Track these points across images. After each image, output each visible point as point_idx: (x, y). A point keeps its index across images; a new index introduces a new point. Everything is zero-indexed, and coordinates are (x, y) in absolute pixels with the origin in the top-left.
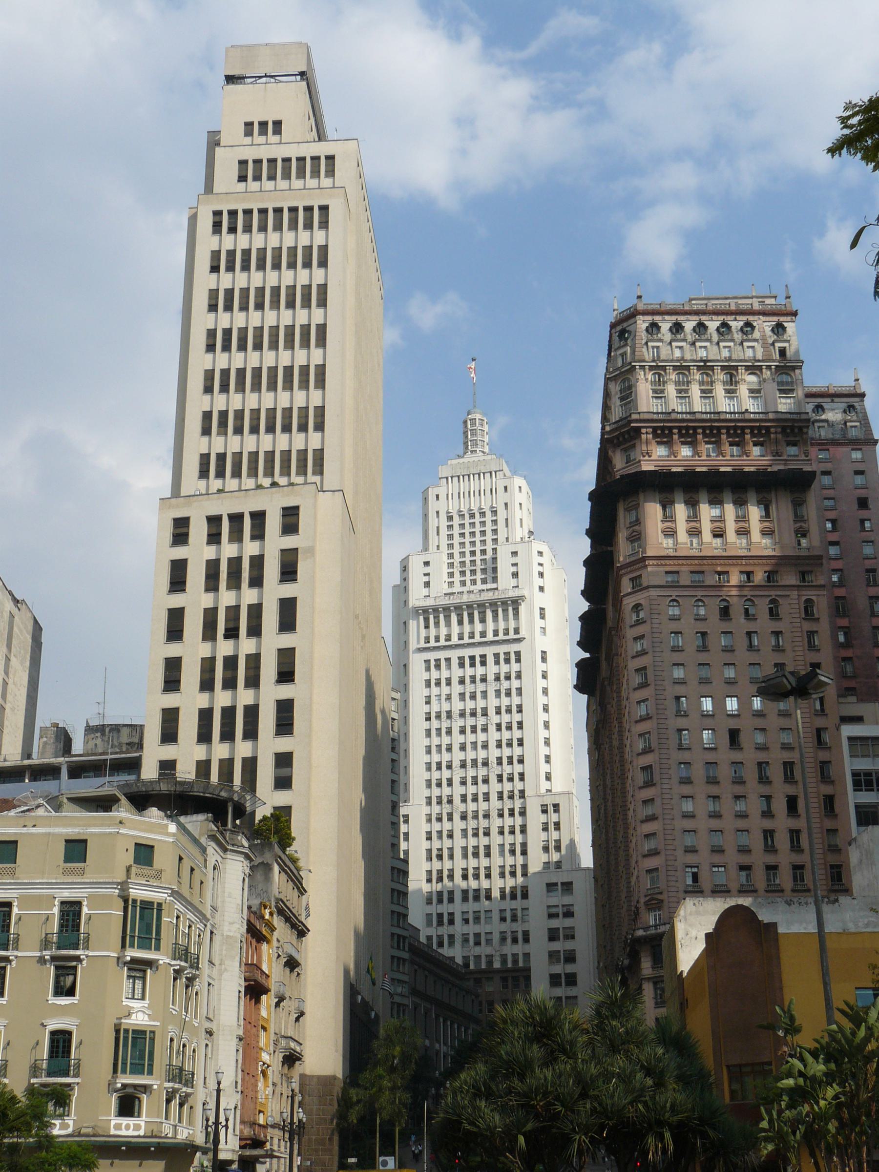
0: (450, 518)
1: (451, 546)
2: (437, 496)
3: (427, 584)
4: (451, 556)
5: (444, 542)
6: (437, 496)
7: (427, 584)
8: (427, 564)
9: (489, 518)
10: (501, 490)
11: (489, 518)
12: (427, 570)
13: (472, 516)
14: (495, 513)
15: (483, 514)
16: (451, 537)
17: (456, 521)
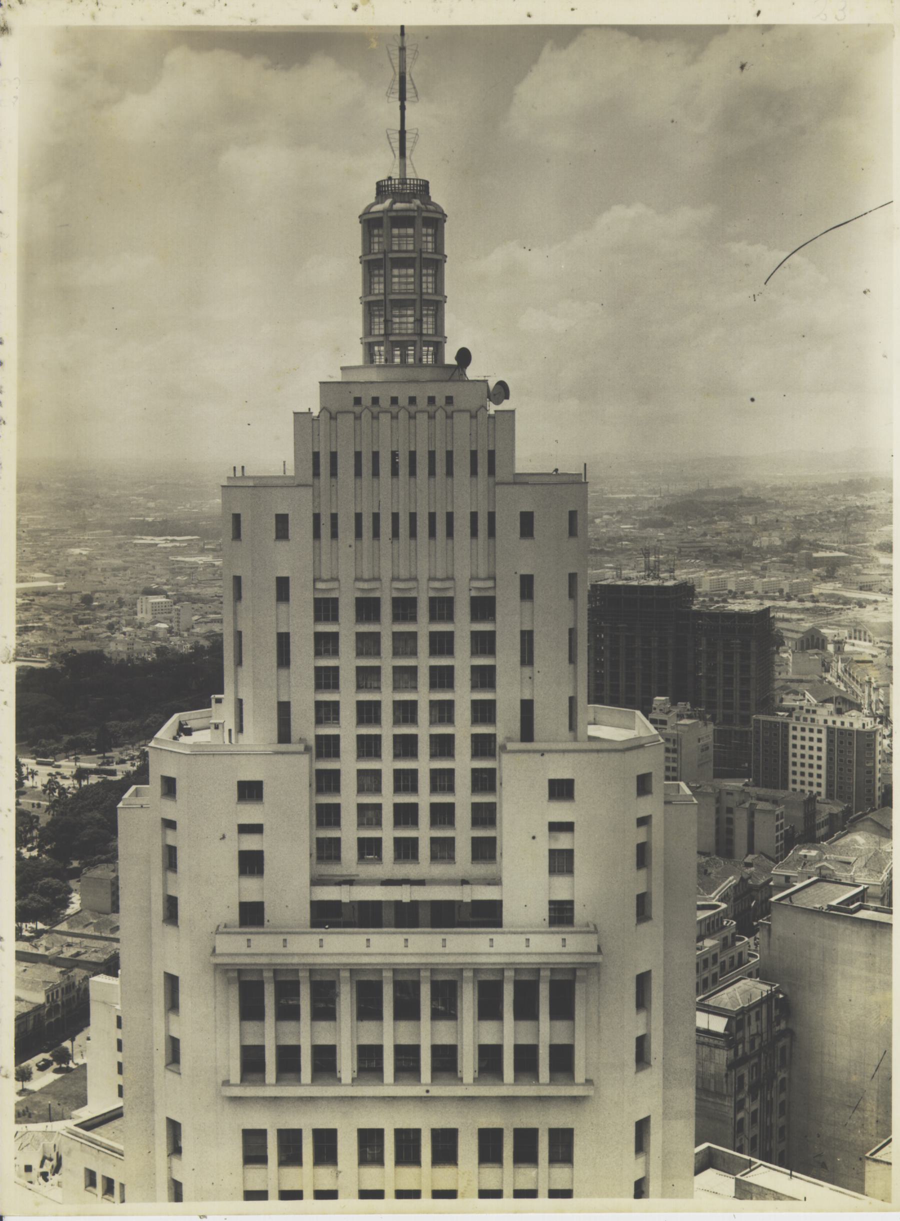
0: (326, 609)
1: (327, 712)
2: (282, 521)
3: (251, 864)
4: (328, 747)
5: (304, 698)
6: (282, 521)
7: (251, 864)
8: (250, 791)
9: (463, 627)
10: (508, 526)
11: (463, 627)
12: (251, 814)
13: (405, 608)
14: (483, 608)
15: (442, 608)
16: (327, 679)
17: (347, 627)
